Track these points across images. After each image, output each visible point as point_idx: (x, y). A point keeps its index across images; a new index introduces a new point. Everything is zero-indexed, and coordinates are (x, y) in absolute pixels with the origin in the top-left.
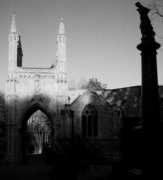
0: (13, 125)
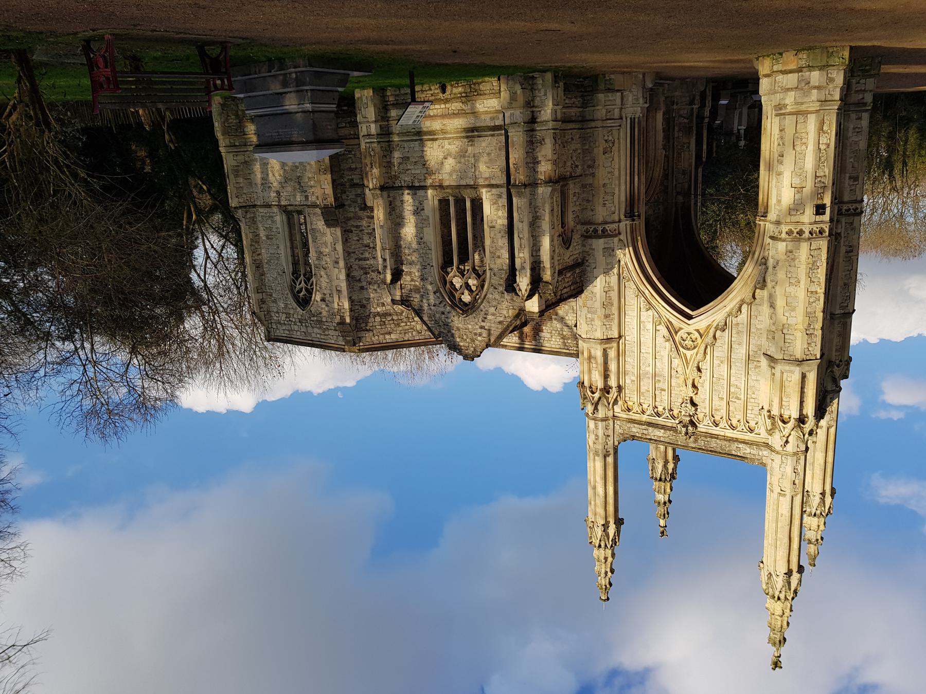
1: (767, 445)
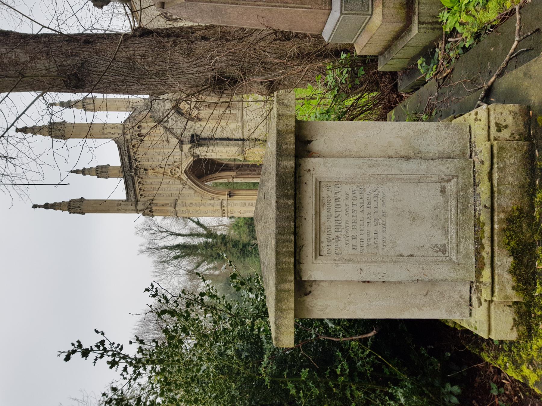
0: (223, 208)
1: (137, 201)
